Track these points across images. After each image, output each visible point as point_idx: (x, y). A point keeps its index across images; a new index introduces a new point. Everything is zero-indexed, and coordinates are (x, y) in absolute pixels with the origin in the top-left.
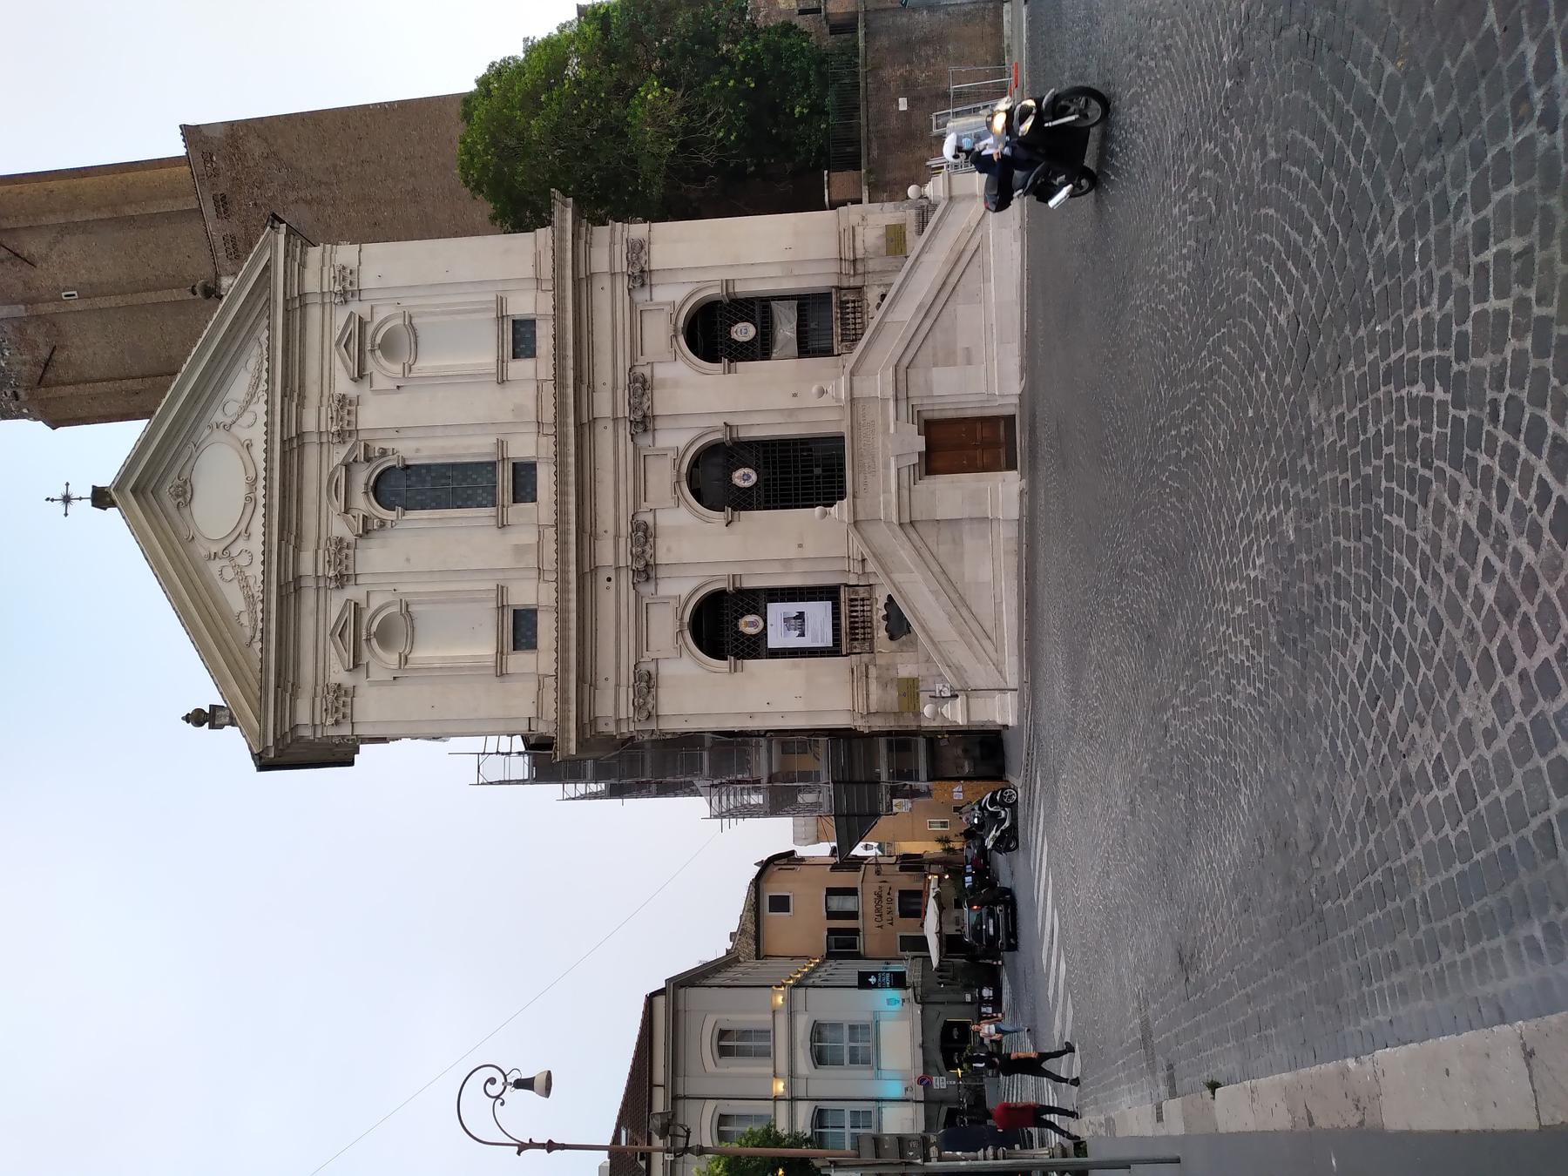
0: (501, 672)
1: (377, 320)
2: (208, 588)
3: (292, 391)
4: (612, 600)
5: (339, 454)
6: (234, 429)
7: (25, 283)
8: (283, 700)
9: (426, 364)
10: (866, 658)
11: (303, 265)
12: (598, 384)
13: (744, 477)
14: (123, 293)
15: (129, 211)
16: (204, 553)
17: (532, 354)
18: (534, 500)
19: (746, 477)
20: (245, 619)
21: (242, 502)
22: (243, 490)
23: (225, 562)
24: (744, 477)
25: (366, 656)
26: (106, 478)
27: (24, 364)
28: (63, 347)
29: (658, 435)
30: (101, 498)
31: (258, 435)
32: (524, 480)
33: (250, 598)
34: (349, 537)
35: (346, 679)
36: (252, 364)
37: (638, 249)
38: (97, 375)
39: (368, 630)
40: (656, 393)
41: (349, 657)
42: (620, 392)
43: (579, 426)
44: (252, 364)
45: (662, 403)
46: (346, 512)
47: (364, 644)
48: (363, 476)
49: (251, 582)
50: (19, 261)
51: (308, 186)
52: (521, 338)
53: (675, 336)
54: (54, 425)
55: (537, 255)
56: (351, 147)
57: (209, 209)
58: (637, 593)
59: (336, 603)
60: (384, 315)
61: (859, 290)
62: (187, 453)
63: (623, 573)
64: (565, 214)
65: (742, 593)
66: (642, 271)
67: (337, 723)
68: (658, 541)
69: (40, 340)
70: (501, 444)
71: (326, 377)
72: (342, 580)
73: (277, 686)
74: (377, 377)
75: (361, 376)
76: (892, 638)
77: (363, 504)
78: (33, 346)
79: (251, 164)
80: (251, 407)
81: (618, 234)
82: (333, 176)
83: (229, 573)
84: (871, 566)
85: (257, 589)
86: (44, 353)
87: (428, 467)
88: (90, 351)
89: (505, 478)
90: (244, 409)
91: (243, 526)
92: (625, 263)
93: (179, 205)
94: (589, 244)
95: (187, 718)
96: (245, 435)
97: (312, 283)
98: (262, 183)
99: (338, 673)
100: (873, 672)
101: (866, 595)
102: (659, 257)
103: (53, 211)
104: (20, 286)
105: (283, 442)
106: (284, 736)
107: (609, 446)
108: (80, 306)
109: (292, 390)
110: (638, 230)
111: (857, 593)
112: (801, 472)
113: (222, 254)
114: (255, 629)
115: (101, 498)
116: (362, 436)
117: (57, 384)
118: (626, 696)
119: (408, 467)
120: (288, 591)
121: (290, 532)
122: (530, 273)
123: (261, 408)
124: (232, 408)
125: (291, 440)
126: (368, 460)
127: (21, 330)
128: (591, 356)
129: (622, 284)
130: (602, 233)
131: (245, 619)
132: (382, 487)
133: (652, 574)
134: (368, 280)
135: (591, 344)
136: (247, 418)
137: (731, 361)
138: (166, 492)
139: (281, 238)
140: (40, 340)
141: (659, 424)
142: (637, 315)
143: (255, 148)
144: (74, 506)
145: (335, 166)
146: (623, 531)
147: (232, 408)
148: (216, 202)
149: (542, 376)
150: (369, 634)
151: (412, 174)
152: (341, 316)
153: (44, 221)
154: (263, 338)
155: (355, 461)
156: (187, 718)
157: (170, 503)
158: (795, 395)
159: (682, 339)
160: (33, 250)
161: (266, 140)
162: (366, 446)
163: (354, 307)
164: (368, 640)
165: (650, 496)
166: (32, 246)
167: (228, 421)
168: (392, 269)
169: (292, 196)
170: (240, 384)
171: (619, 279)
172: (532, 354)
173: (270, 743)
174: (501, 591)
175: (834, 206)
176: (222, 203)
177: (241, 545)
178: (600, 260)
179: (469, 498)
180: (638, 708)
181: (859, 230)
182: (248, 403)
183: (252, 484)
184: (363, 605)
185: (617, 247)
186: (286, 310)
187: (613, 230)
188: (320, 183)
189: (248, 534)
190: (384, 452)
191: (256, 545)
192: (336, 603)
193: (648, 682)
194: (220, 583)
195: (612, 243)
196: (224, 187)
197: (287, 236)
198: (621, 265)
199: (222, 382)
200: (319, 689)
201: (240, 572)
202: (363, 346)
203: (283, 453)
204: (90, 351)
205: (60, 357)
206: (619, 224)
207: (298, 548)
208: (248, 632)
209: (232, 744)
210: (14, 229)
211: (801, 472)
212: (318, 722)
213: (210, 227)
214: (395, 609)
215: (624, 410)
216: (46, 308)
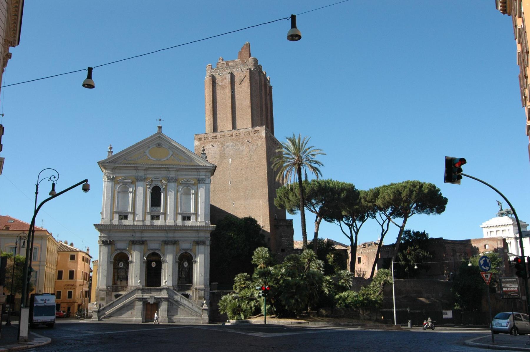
13: (154, 264)
24: (154, 264)
26: (163, 131)
30: (160, 128)
37: (203, 243)
48: (159, 184)
69: (223, 84)
130: (208, 235)
144: (158, 122)
151: (252, 180)
175: (210, 284)
209: (105, 156)
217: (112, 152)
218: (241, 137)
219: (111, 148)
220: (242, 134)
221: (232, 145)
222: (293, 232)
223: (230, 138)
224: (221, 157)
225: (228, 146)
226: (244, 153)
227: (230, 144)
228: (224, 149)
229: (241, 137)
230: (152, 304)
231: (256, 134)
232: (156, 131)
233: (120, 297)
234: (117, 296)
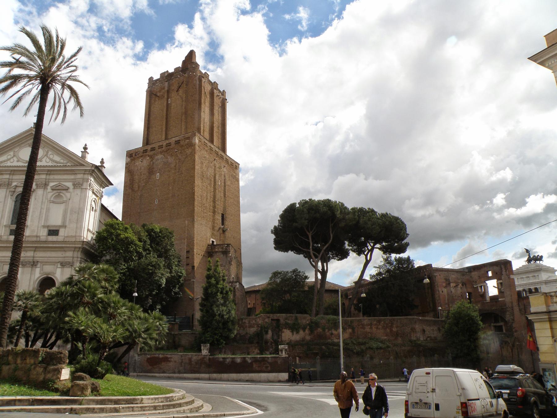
2: (6, 152)
9: (53, 207)
44: (62, 161)
52: (53, 232)
74: (52, 193)
75: (52, 189)
78: (160, 91)
83: (9, 157)
86: (158, 94)
122: (70, 234)
123: (50, 164)
128: (44, 251)
135: (48, 251)
136: (48, 160)
142: (54, 263)
143: (189, 151)
151: (178, 195)
152: (69, 185)
159: (45, 276)
166: (181, 91)
169: (177, 161)
170: (57, 158)
178: (70, 254)
189: (18, 161)
191: (16, 164)
196: (182, 143)
198: (67, 260)
199: (58, 154)
213: (174, 139)
220: (173, 145)
223: (160, 150)
224: (149, 173)
225: (158, 160)
227: (160, 156)
228: (153, 163)
229: (171, 147)
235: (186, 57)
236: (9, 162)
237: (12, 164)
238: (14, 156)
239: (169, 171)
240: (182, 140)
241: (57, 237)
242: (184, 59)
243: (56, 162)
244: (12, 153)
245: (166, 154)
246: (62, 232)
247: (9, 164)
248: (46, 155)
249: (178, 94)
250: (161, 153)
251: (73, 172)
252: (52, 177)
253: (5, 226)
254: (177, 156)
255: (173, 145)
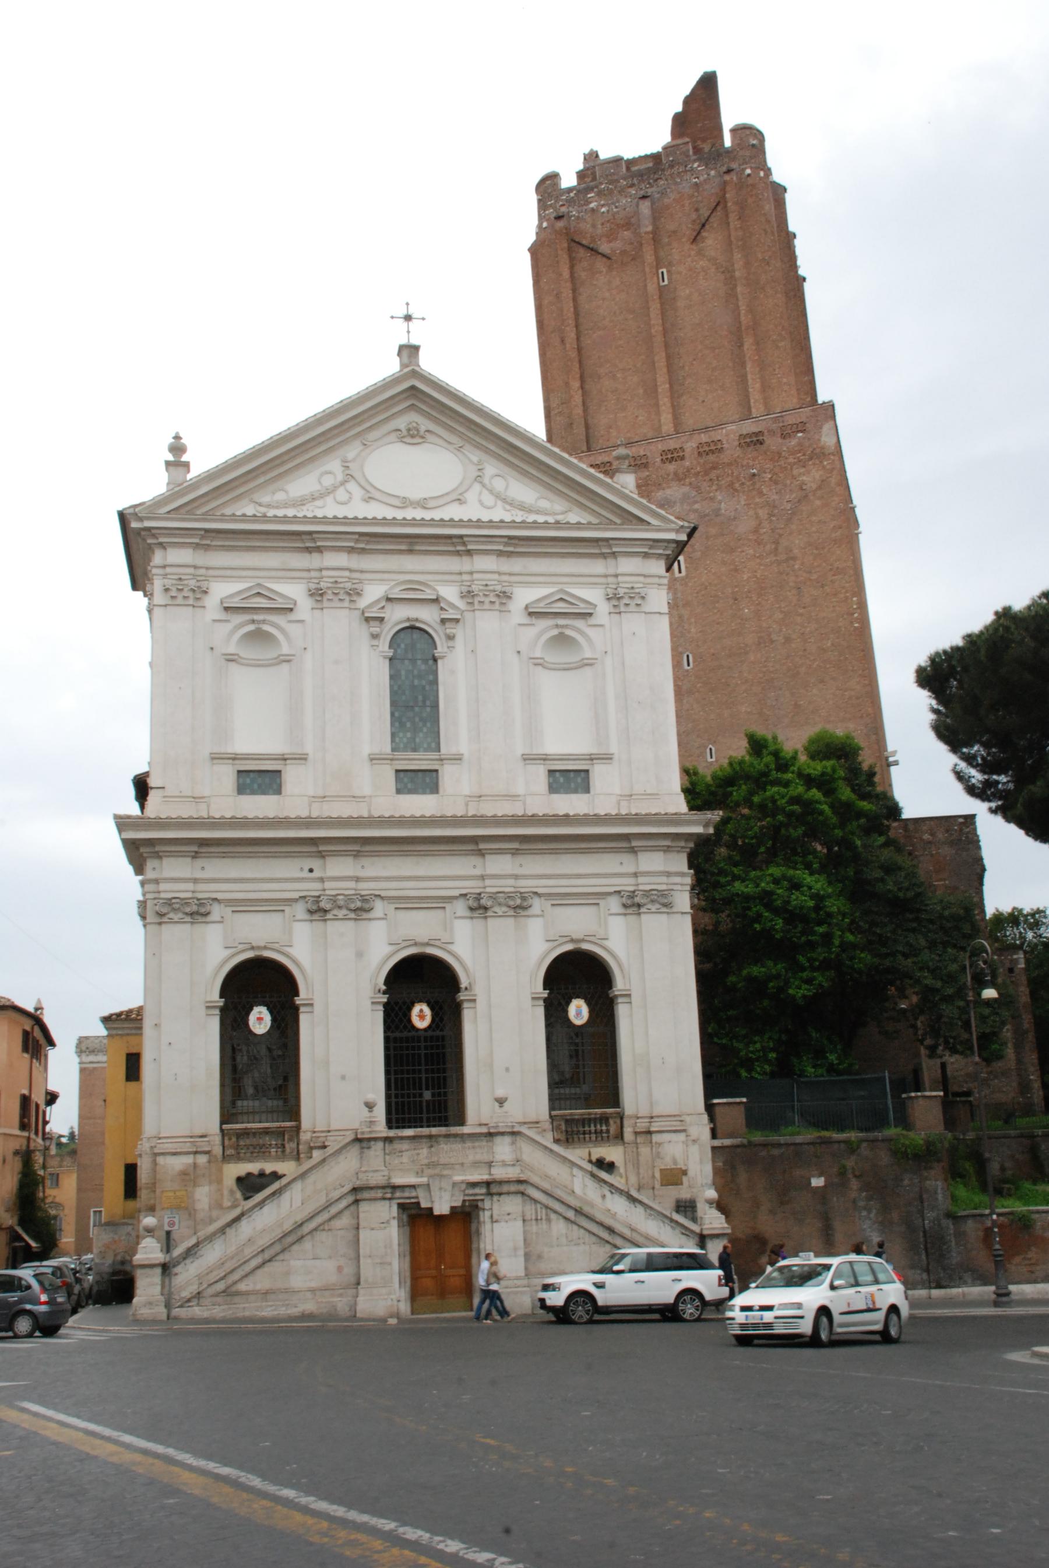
0: (216, 758)
1: (591, 632)
2: (312, 460)
3: (515, 545)
4: (287, 875)
5: (450, 593)
6: (477, 487)
7: (674, 232)
8: (192, 536)
10: (218, 1150)
11: (646, 555)
12: (520, 859)
13: (421, 1016)
14: (665, 332)
15: (748, 343)
16: (350, 455)
17: (553, 789)
18: (399, 791)
19: (422, 1017)
20: (280, 496)
21: (402, 495)
22: (416, 495)
23: (340, 477)
24: (421, 1016)
25: (238, 619)
26: (427, 363)
27: (594, 226)
28: (610, 268)
29: (468, 922)
30: (408, 351)
31: (470, 511)
32: (420, 780)
33: (302, 502)
34: (363, 603)
35: (212, 601)
36: (544, 504)
38: (582, 299)
39: (264, 622)
40: (511, 920)
41: (235, 602)
42: (511, 882)
43: (474, 840)
44: (544, 504)
45: (501, 926)
46: (389, 600)
47: (247, 617)
48: (427, 616)
49: (318, 503)
50: (698, 227)
51: (773, 530)
53: (572, 941)
54: (535, 251)
55: (654, 796)
56: (814, 577)
57: (749, 427)
58: (296, 900)
59: (295, 591)
60: (598, 636)
61: (620, 1136)
62: (453, 439)
63: (318, 885)
64: (700, 825)
65: (295, 1010)
66: (639, 906)
67: (167, 590)
68: (351, 924)
69: (618, 245)
70: (458, 758)
71: (530, 579)
72: (317, 594)
73: (207, 531)
74: (531, 632)
76: (239, 1180)
77: (398, 615)
78: (611, 236)
79: (795, 472)
80: (499, 503)
81: (678, 880)
82: (783, 557)
83: (328, 481)
84: (317, 1155)
85: (308, 511)
86: (604, 247)
87: (435, 682)
88: (607, 294)
89: (420, 761)
90: (498, 496)
91: (377, 495)
92: (648, 887)
93: (755, 395)
94: (667, 849)
95: (177, 437)
96: (471, 496)
97: (627, 565)
98: (776, 483)
99: (221, 590)
100: (202, 1159)
101: (288, 1150)
102: (653, 922)
103: (747, 264)
104: (671, 226)
105: (461, 537)
106: (154, 536)
107: (455, 872)
108: (652, 288)
109: (518, 544)
110: (683, 900)
111: (291, 1140)
112: (424, 1077)
113: (704, 438)
114: (269, 506)
115: (408, 351)
116: (468, 615)
117: (572, 259)
118: (184, 890)
119: (435, 660)
120: (306, 540)
121: (368, 542)
123: (499, 513)
124: (499, 484)
125: (464, 544)
126: (443, 621)
127: (627, 225)
129: (627, 884)
130: (680, 863)
131: (280, 496)
132: (416, 635)
133: (316, 917)
134: (632, 622)
135: (567, 851)
136: (489, 499)
137: (545, 1000)
138: (413, 417)
139: (672, 536)
140: (618, 245)
141: (479, 923)
142: (594, 899)
144: (402, 325)
145: (794, 559)
146: (362, 885)
147: (499, 484)
148: (756, 434)
149: (529, 800)
150: (259, 622)
151: (788, 640)
152: (594, 595)
153: (737, 256)
154: (573, 518)
155: (442, 609)
156: (177, 437)
157: (402, 423)
158: (507, 1070)
159: (569, 947)
160: (709, 242)
161: (819, 488)
162: (457, 621)
163: (603, 608)
164: (253, 621)
165: (401, 914)
166: (712, 241)
167: (486, 481)
168: (639, 649)
169: (763, 513)
170: (524, 492)
171: (632, 881)
172: (553, 789)
173: (147, 524)
174: (303, 758)
175: (709, 1108)
176: (754, 441)
177: (357, 493)
178: (653, 862)
179: (402, 725)
180: (169, 902)
181: (682, 1137)
182: (504, 500)
183: (422, 504)
184: (292, 616)
185: (664, 879)
186: (597, 540)
187: (682, 875)
188: (777, 543)
189: (369, 499)
190: (451, 638)
192: (295, 591)
193: (197, 913)
194: (317, 473)
195: (668, 874)
196: (773, 443)
197: (677, 542)
198: (646, 884)
199: (525, 473)
200: (202, 571)
201: (330, 491)
202: (562, 618)
203: (450, 537)
204: (607, 294)
205: (600, 264)
206: (689, 880)
207: (351, 550)
208: (266, 499)
209: (149, 484)
210: (728, 224)
211: (424, 1077)
212: (168, 570)
213: (732, 427)
214: (285, 649)
215: (492, 886)
216: (649, 257)
217: (186, 465)
218: (725, 458)
219: (177, 448)
220: (731, 450)
221: (685, 498)
222: (983, 869)
223: (671, 467)
226: (744, 526)
229: (725, 458)
230: (441, 1218)
231: (794, 442)
232: (392, 366)
233: (276, 1186)
234: (250, 1185)
235: (687, 101)
236: (329, 499)
237: (341, 512)
238: (350, 477)
239: (732, 550)
240: (772, 432)
241: (273, 798)
242: (679, 108)
243: (522, 507)
244: (334, 465)
245: (705, 486)
246: (602, 777)
247: (329, 509)
248: (479, 479)
249: (700, 253)
250: (679, 478)
251: (603, 549)
252: (517, 565)
253: (373, 759)
254: (761, 493)
255: (731, 450)
